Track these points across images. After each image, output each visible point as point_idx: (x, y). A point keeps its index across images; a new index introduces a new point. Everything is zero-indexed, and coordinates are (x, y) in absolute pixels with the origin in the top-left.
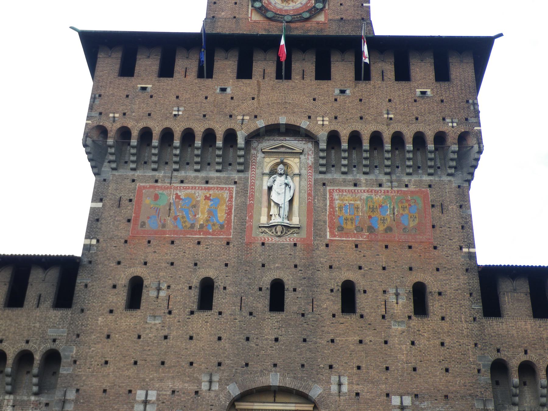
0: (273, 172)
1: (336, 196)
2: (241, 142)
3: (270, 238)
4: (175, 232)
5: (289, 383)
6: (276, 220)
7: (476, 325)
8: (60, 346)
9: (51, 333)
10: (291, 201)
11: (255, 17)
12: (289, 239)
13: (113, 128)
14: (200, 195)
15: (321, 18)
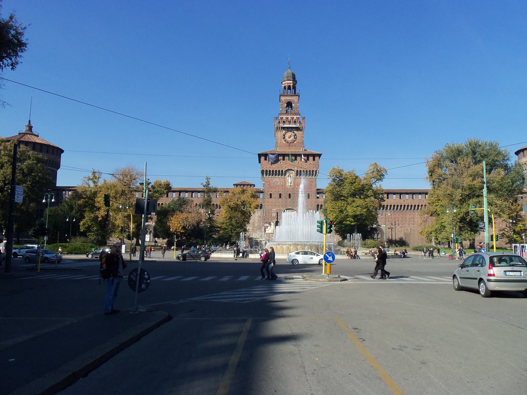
0: (288, 176)
1: (298, 180)
2: (284, 172)
3: (289, 187)
4: (276, 186)
5: (292, 208)
6: (289, 185)
7: (315, 200)
8: (262, 203)
9: (261, 202)
10: (291, 182)
11: (284, 142)
12: (291, 187)
13: (265, 170)
14: (278, 180)
15: (295, 142)
